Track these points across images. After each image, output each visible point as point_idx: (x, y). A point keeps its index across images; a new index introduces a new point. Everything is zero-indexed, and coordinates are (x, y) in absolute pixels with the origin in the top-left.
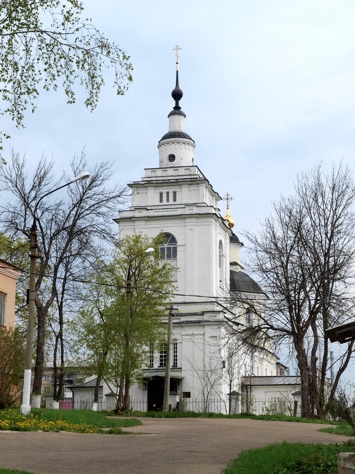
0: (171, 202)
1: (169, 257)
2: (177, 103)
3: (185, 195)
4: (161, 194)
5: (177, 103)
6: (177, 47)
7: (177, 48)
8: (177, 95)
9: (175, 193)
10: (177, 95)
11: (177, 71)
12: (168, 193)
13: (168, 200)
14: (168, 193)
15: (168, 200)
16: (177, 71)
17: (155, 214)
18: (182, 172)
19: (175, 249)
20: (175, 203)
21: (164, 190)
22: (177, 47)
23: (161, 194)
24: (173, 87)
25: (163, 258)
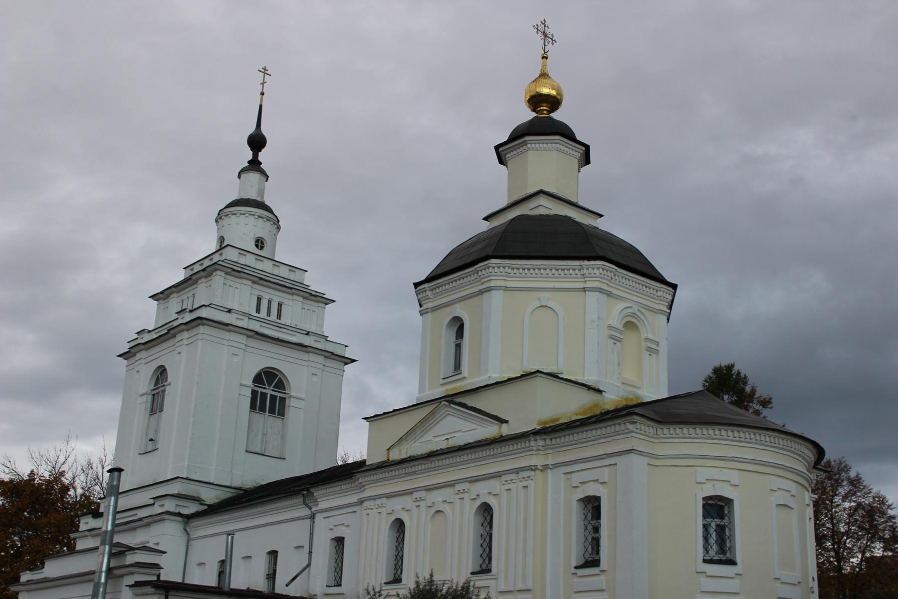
0: (274, 316)
1: (272, 411)
2: (255, 155)
3: (295, 312)
4: (259, 299)
5: (255, 155)
6: (265, 69)
7: (264, 71)
8: (257, 142)
9: (280, 305)
10: (257, 142)
11: (261, 106)
12: (270, 302)
13: (269, 314)
14: (270, 302)
15: (269, 314)
16: (261, 106)
17: (294, 339)
18: (267, 266)
19: (283, 400)
20: (278, 321)
21: (267, 294)
22: (265, 69)
23: (259, 299)
24: (252, 129)
25: (262, 409)
